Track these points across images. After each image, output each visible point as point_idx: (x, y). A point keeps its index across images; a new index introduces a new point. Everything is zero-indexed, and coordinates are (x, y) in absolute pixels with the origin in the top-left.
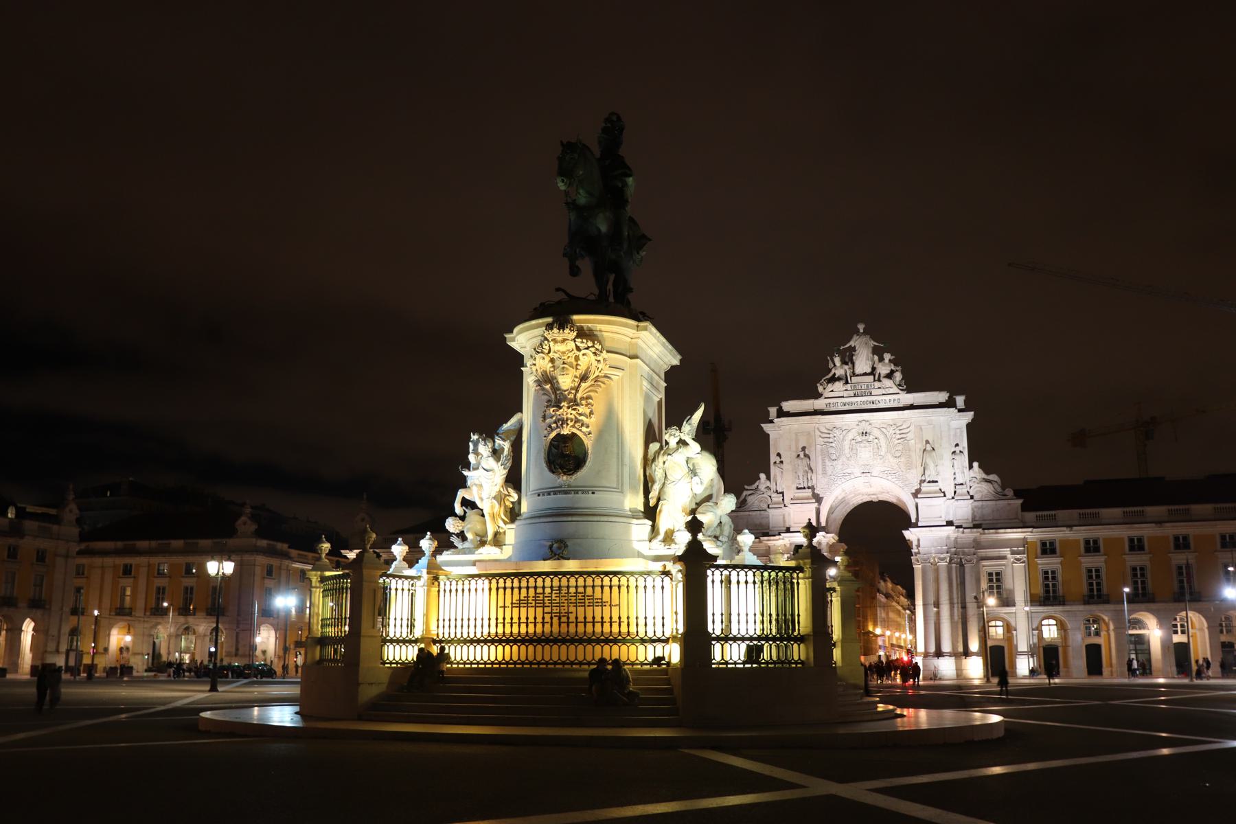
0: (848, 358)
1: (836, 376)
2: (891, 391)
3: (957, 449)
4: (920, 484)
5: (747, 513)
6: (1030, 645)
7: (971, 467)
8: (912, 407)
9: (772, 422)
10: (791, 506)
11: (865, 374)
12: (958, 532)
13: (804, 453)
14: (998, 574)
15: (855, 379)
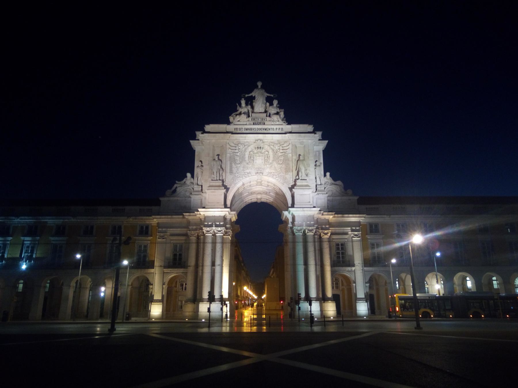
0: (250, 101)
1: (242, 113)
2: (278, 123)
3: (318, 163)
4: (295, 181)
5: (176, 198)
6: (365, 294)
7: (325, 175)
8: (290, 133)
9: (198, 140)
10: (207, 191)
11: (261, 113)
12: (320, 213)
13: (219, 158)
14: (342, 245)
15: (254, 115)
